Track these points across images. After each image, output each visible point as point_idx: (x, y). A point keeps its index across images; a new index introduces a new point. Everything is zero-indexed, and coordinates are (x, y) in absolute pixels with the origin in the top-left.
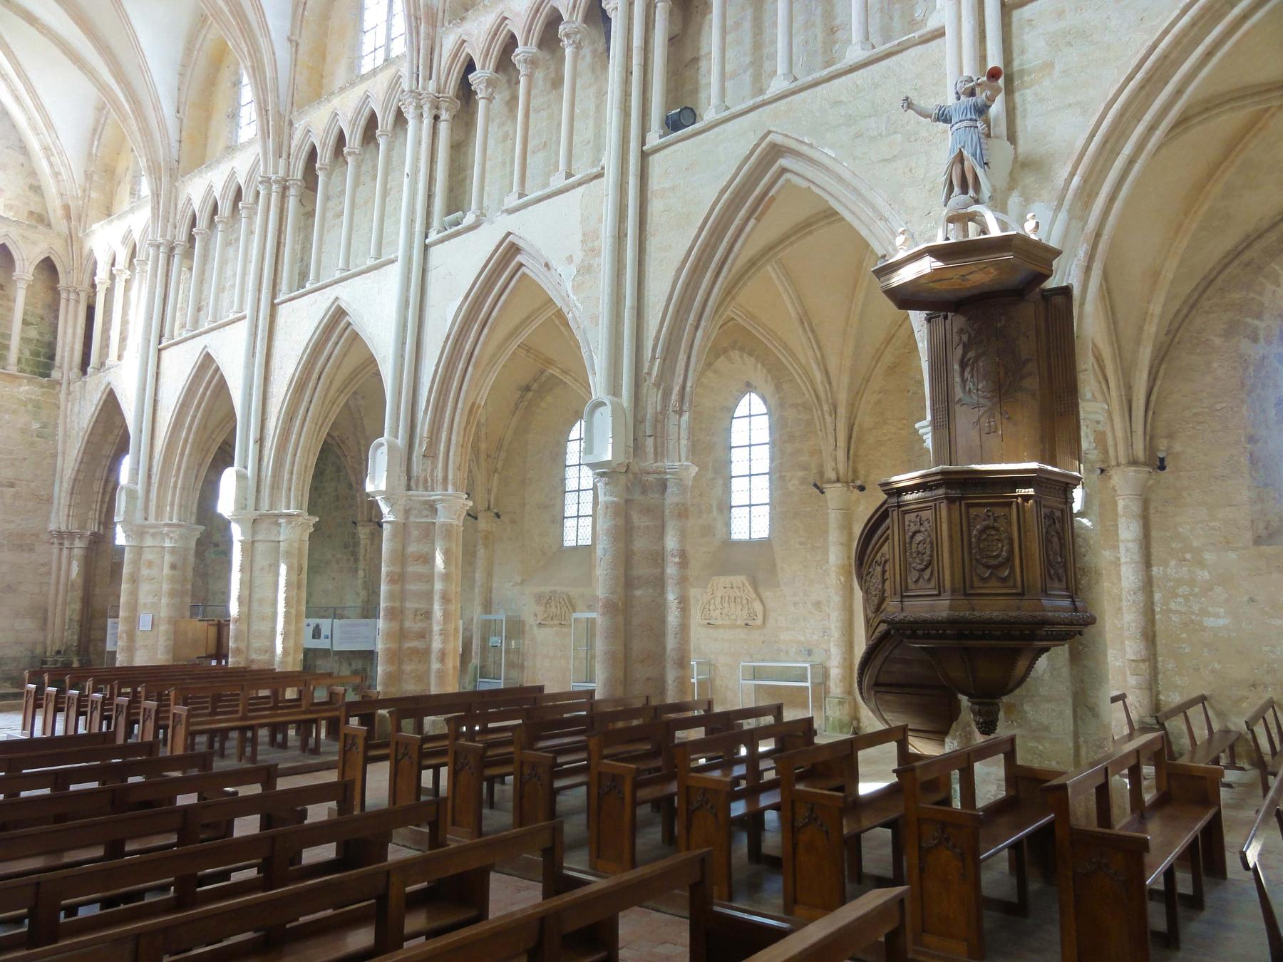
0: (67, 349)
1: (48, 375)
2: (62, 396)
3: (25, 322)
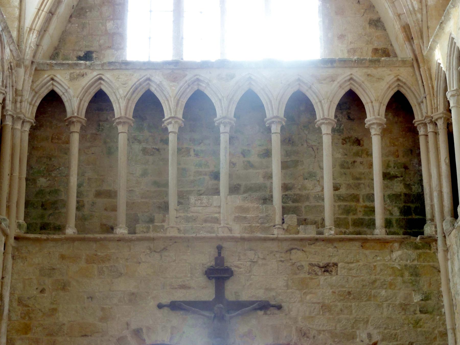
0: (435, 194)
1: (422, 233)
2: (440, 255)
3: (386, 176)
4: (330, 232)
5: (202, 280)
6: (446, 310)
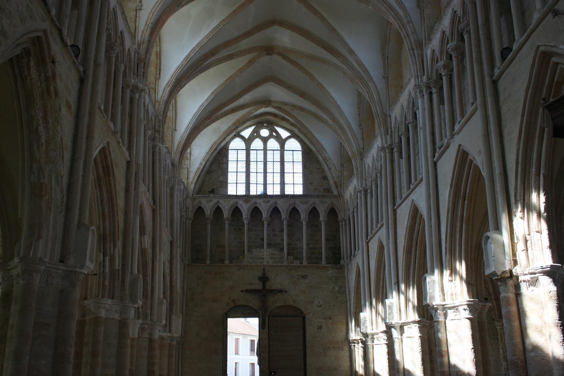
1: (339, 263)
2: (346, 272)
3: (327, 240)
4: (305, 263)
5: (258, 282)
6: (347, 293)
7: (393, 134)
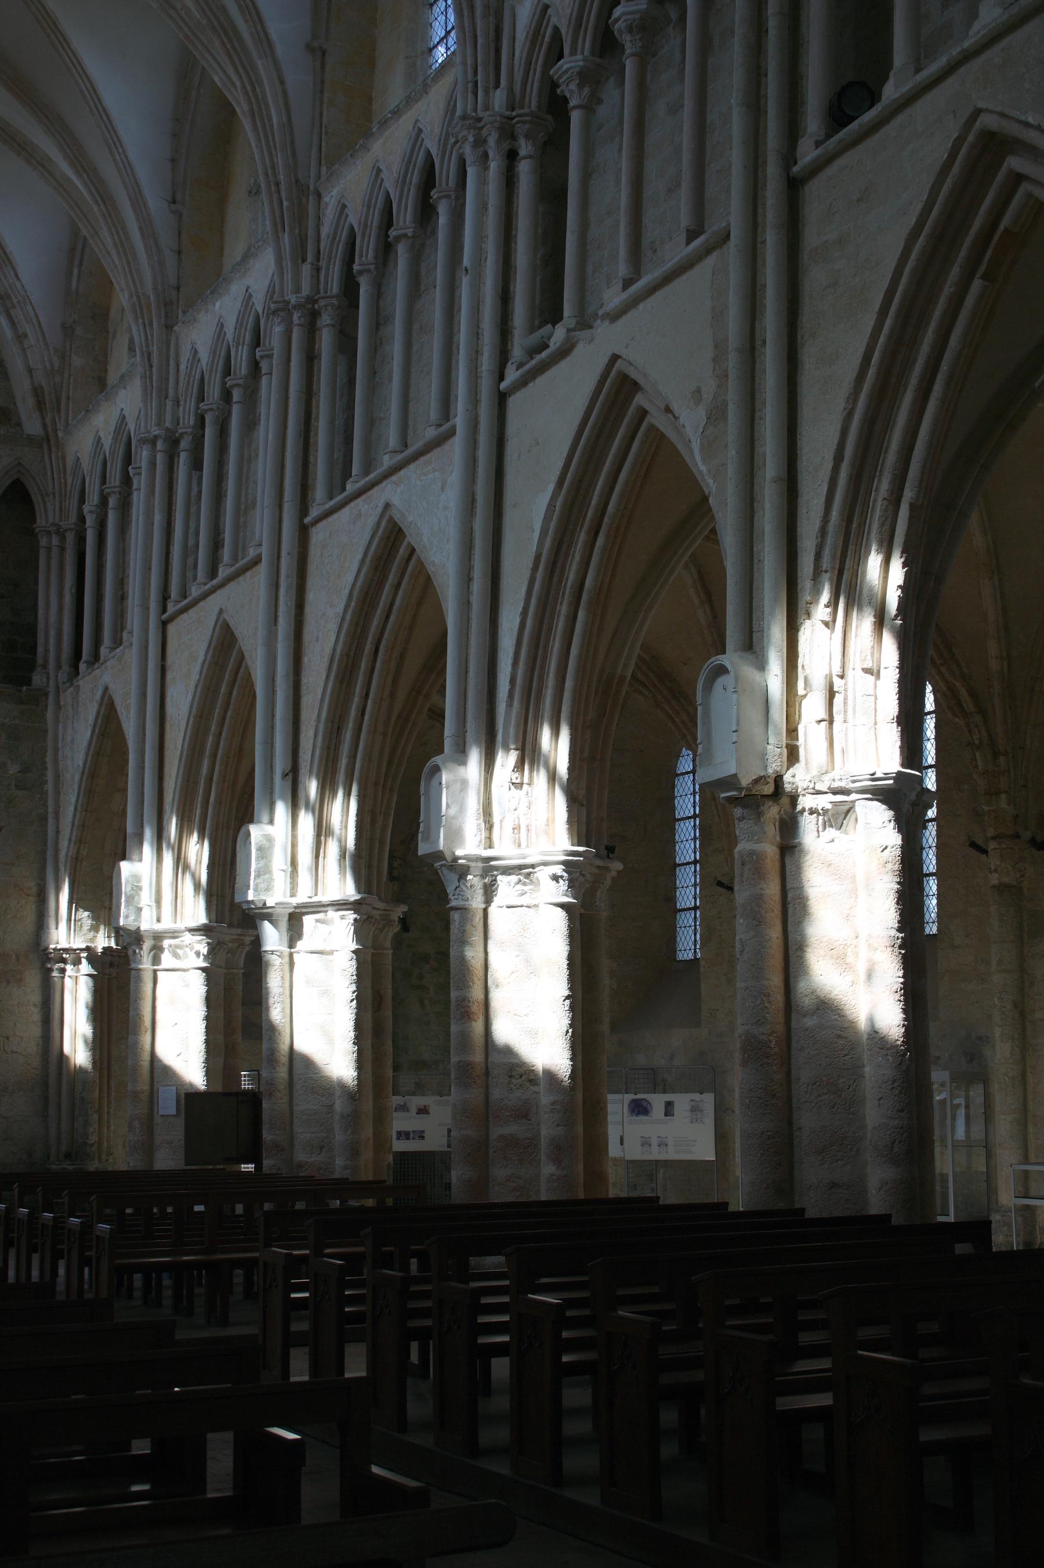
0: (52, 633)
1: (28, 682)
2: (50, 715)
6: (50, 787)
7: (323, 263)
